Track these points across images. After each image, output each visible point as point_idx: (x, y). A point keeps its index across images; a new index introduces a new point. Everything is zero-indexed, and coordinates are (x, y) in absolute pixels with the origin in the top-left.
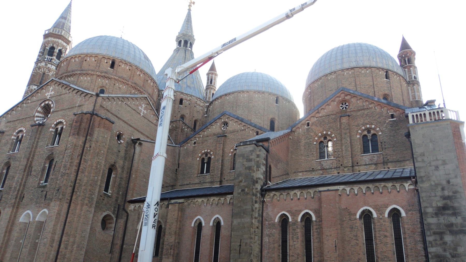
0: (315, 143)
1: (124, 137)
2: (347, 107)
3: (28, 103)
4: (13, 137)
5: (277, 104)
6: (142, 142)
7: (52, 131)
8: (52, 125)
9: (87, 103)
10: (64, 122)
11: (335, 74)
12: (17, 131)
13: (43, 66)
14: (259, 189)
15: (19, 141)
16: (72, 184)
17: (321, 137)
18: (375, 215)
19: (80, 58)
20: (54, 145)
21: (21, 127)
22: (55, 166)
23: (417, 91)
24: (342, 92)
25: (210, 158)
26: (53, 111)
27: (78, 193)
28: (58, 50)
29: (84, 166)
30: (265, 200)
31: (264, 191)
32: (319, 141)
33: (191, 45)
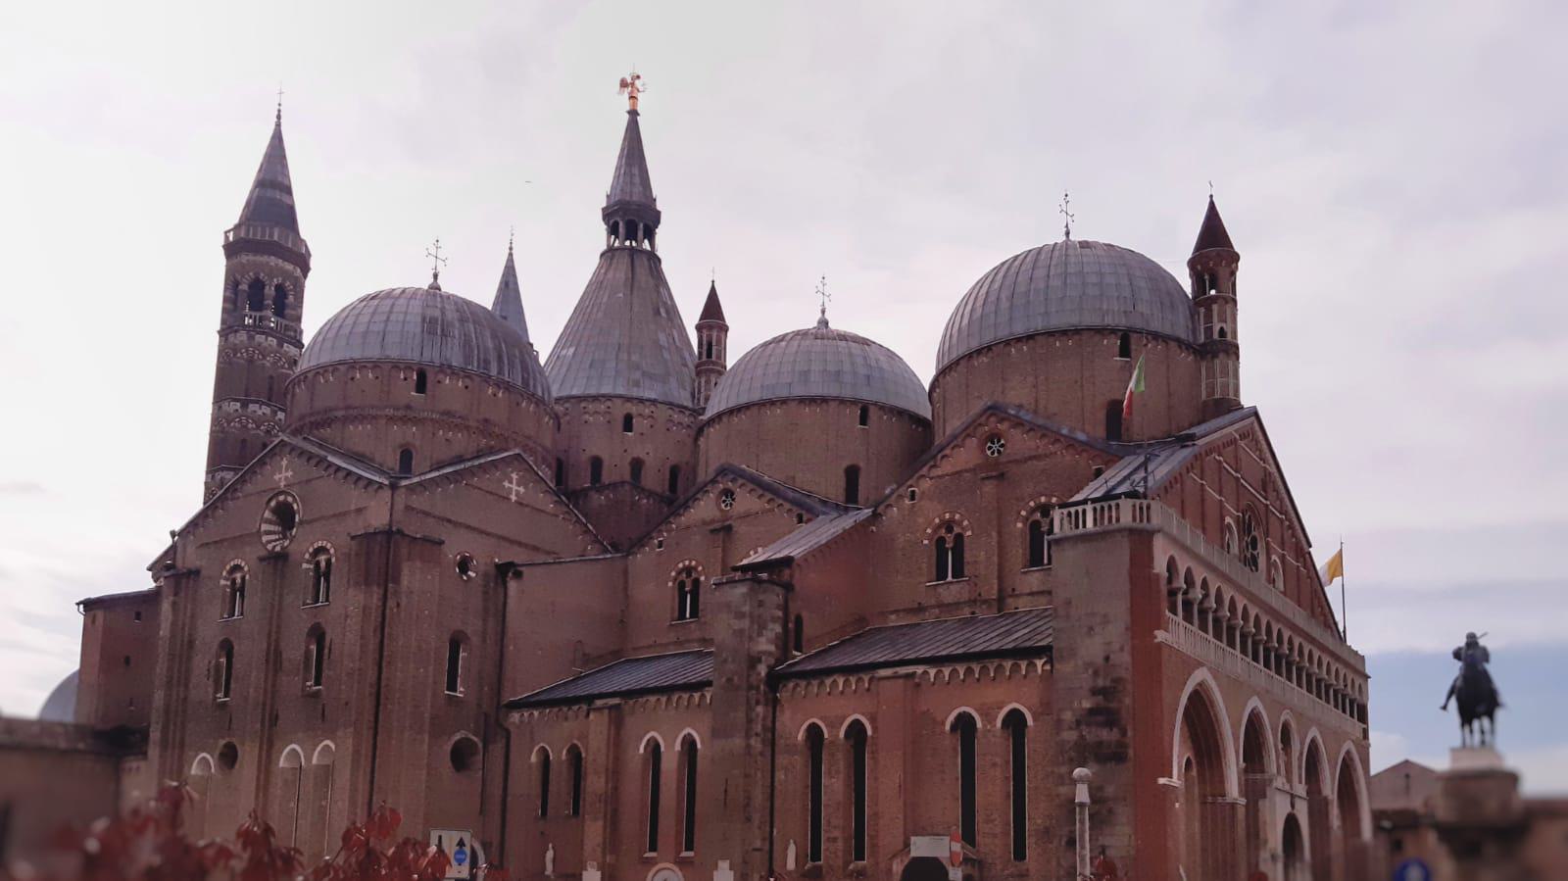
0: (926, 542)
2: (1002, 449)
4: (223, 582)
5: (865, 425)
6: (521, 569)
11: (990, 354)
13: (242, 341)
14: (763, 674)
15: (238, 590)
17: (939, 527)
18: (979, 725)
22: (330, 650)
23: (1221, 372)
24: (989, 412)
25: (696, 582)
28: (273, 288)
30: (778, 695)
31: (775, 680)
32: (936, 537)
33: (650, 234)
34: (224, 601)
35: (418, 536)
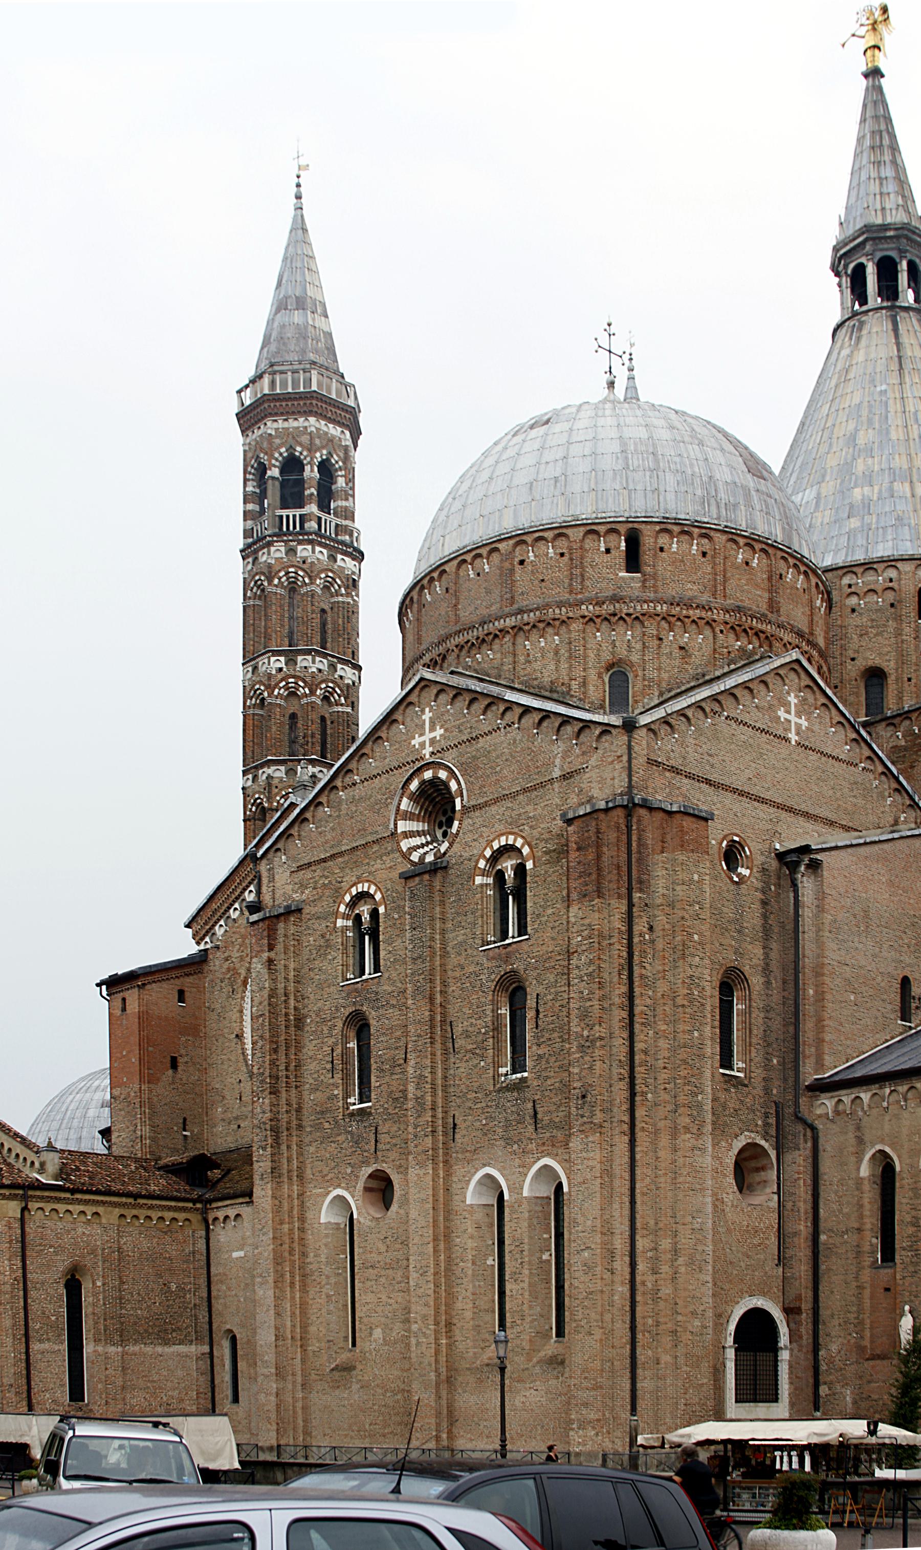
1: (748, 853)
3: (354, 784)
6: (818, 857)
7: (487, 884)
8: (477, 862)
9: (593, 762)
10: (523, 846)
12: (347, 898)
15: (367, 933)
16: (622, 1071)
19: (495, 557)
20: (504, 935)
21: (359, 880)
22: (538, 1012)
26: (463, 806)
27: (650, 1095)
29: (649, 1002)
34: (345, 952)
35: (675, 809)
